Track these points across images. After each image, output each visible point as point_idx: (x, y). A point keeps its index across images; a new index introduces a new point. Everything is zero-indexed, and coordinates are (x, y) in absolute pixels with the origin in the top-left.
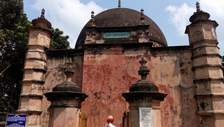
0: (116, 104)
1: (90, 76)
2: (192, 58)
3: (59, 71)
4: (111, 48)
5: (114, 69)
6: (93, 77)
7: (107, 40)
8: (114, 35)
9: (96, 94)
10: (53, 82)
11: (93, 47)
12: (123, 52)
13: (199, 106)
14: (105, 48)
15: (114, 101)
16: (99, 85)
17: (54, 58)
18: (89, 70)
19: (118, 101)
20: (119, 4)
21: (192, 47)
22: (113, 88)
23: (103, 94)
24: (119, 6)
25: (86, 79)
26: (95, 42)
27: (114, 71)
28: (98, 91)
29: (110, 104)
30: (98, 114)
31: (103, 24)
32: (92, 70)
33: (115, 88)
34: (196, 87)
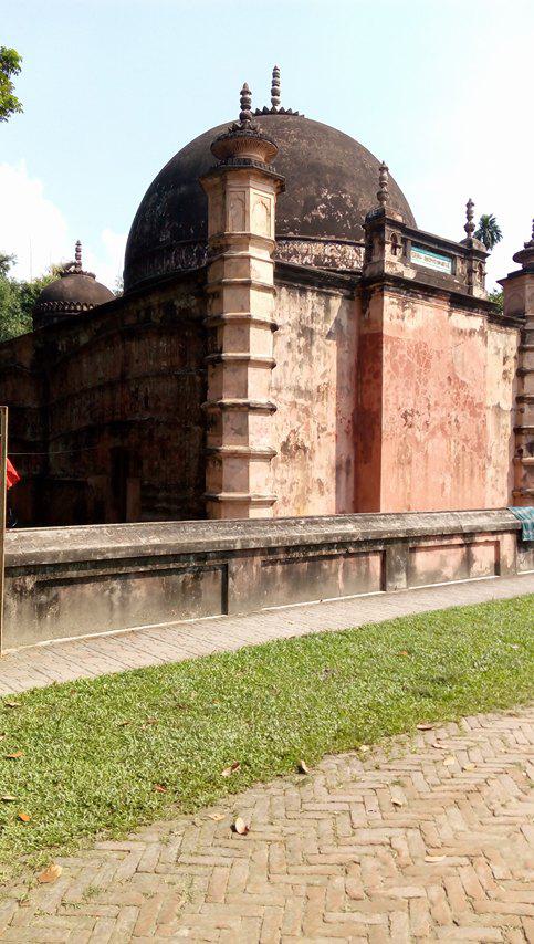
0: (435, 440)
1: (395, 367)
2: (521, 350)
3: (299, 335)
4: (431, 299)
5: (435, 355)
6: (401, 370)
7: (420, 270)
8: (426, 259)
9: (405, 416)
10: (288, 369)
11: (404, 288)
12: (450, 313)
13: (523, 447)
14: (420, 296)
15: (433, 434)
16: (411, 395)
17: (284, 289)
18: (394, 351)
19: (439, 434)
20: (275, 83)
21: (524, 324)
22: (432, 403)
23: (416, 416)
24: (275, 93)
25: (389, 376)
26: (402, 274)
27: (434, 363)
28: (409, 409)
29: (427, 440)
30: (409, 463)
31: (345, 192)
32: (400, 352)
33: (436, 404)
34: (522, 411)
